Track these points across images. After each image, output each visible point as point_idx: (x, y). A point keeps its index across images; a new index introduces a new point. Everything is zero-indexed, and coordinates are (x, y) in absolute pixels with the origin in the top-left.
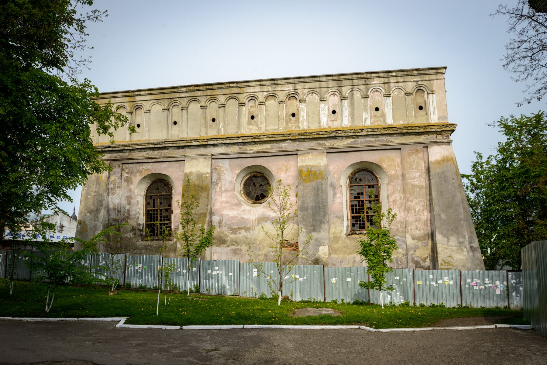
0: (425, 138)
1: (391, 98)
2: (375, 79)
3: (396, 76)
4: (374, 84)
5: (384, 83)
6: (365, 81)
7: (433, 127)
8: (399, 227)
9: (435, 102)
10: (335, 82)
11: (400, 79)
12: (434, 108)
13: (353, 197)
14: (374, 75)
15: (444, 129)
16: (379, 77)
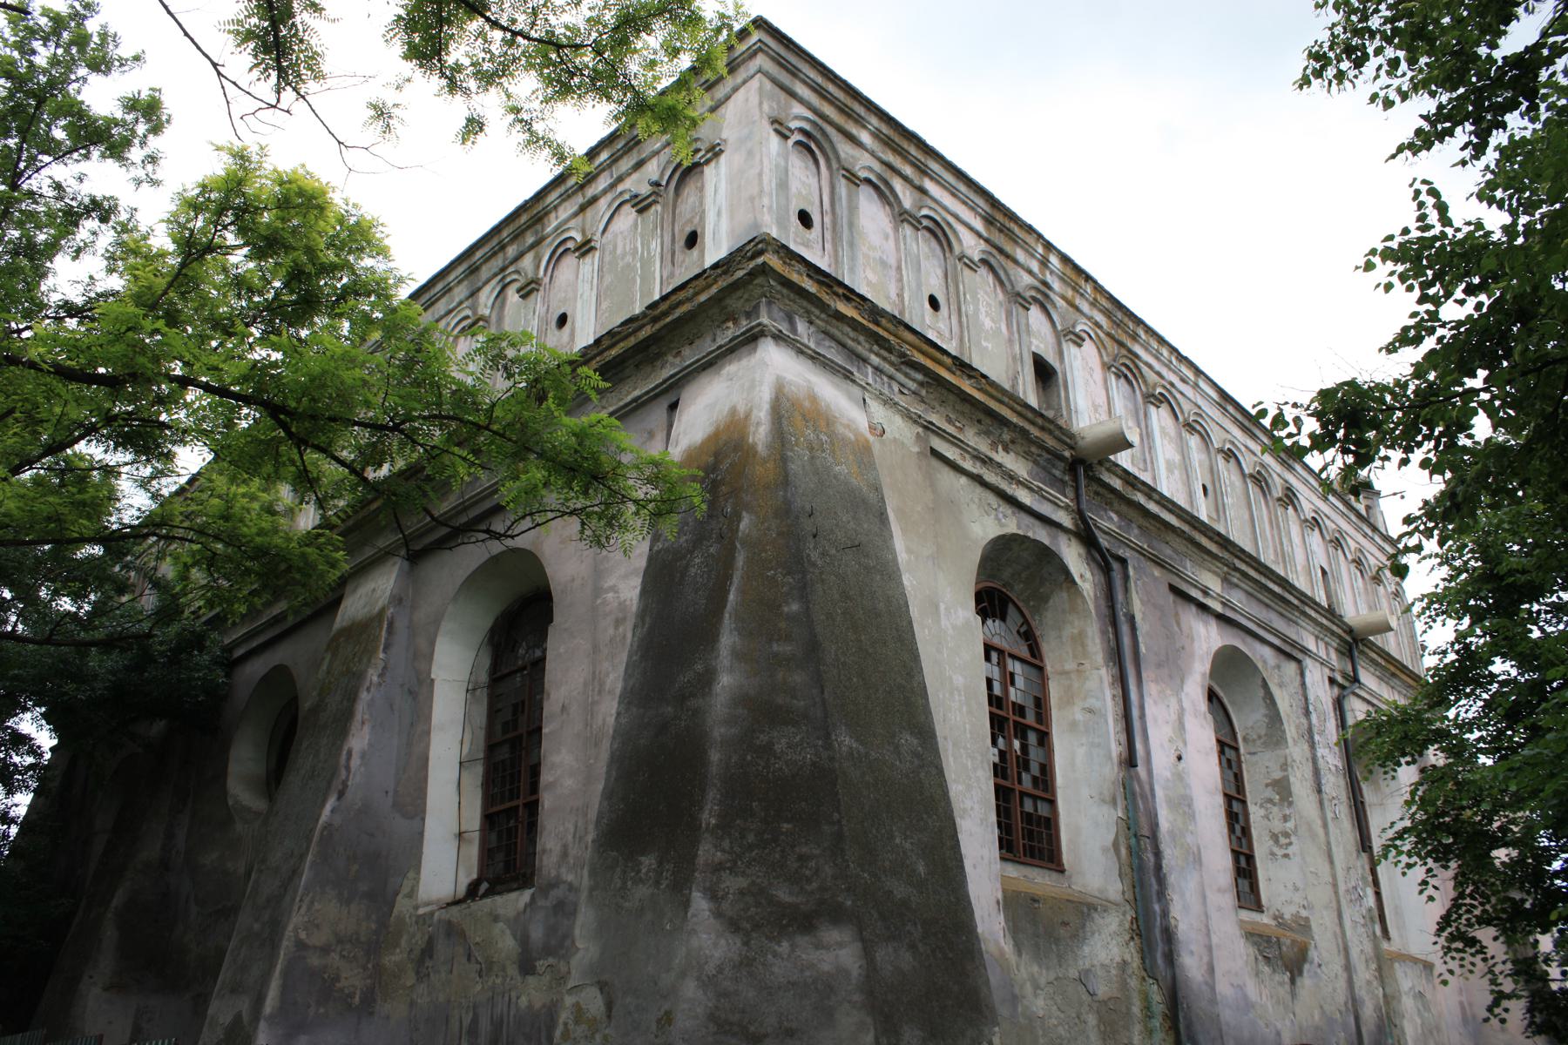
0: (677, 360)
1: (597, 254)
2: (561, 209)
3: (615, 160)
4: (556, 229)
5: (583, 208)
6: (536, 233)
7: (682, 295)
8: (570, 837)
9: (723, 186)
10: (465, 283)
11: (625, 164)
12: (719, 214)
13: (498, 728)
14: (552, 197)
15: (722, 283)
16: (566, 197)
